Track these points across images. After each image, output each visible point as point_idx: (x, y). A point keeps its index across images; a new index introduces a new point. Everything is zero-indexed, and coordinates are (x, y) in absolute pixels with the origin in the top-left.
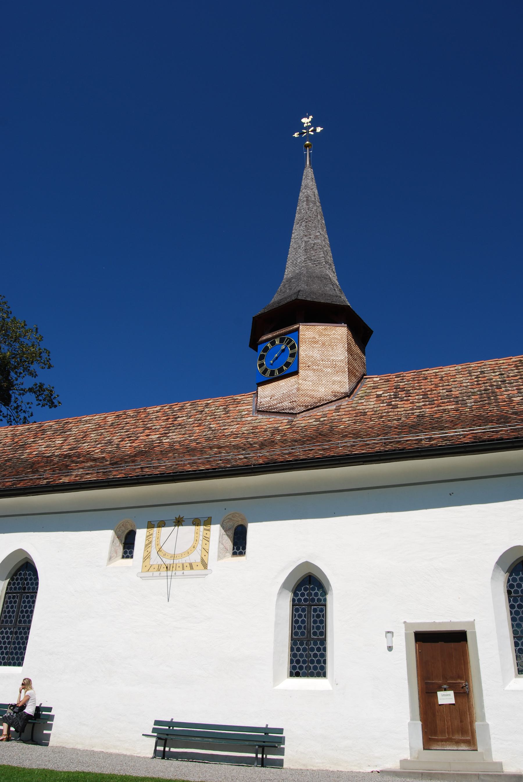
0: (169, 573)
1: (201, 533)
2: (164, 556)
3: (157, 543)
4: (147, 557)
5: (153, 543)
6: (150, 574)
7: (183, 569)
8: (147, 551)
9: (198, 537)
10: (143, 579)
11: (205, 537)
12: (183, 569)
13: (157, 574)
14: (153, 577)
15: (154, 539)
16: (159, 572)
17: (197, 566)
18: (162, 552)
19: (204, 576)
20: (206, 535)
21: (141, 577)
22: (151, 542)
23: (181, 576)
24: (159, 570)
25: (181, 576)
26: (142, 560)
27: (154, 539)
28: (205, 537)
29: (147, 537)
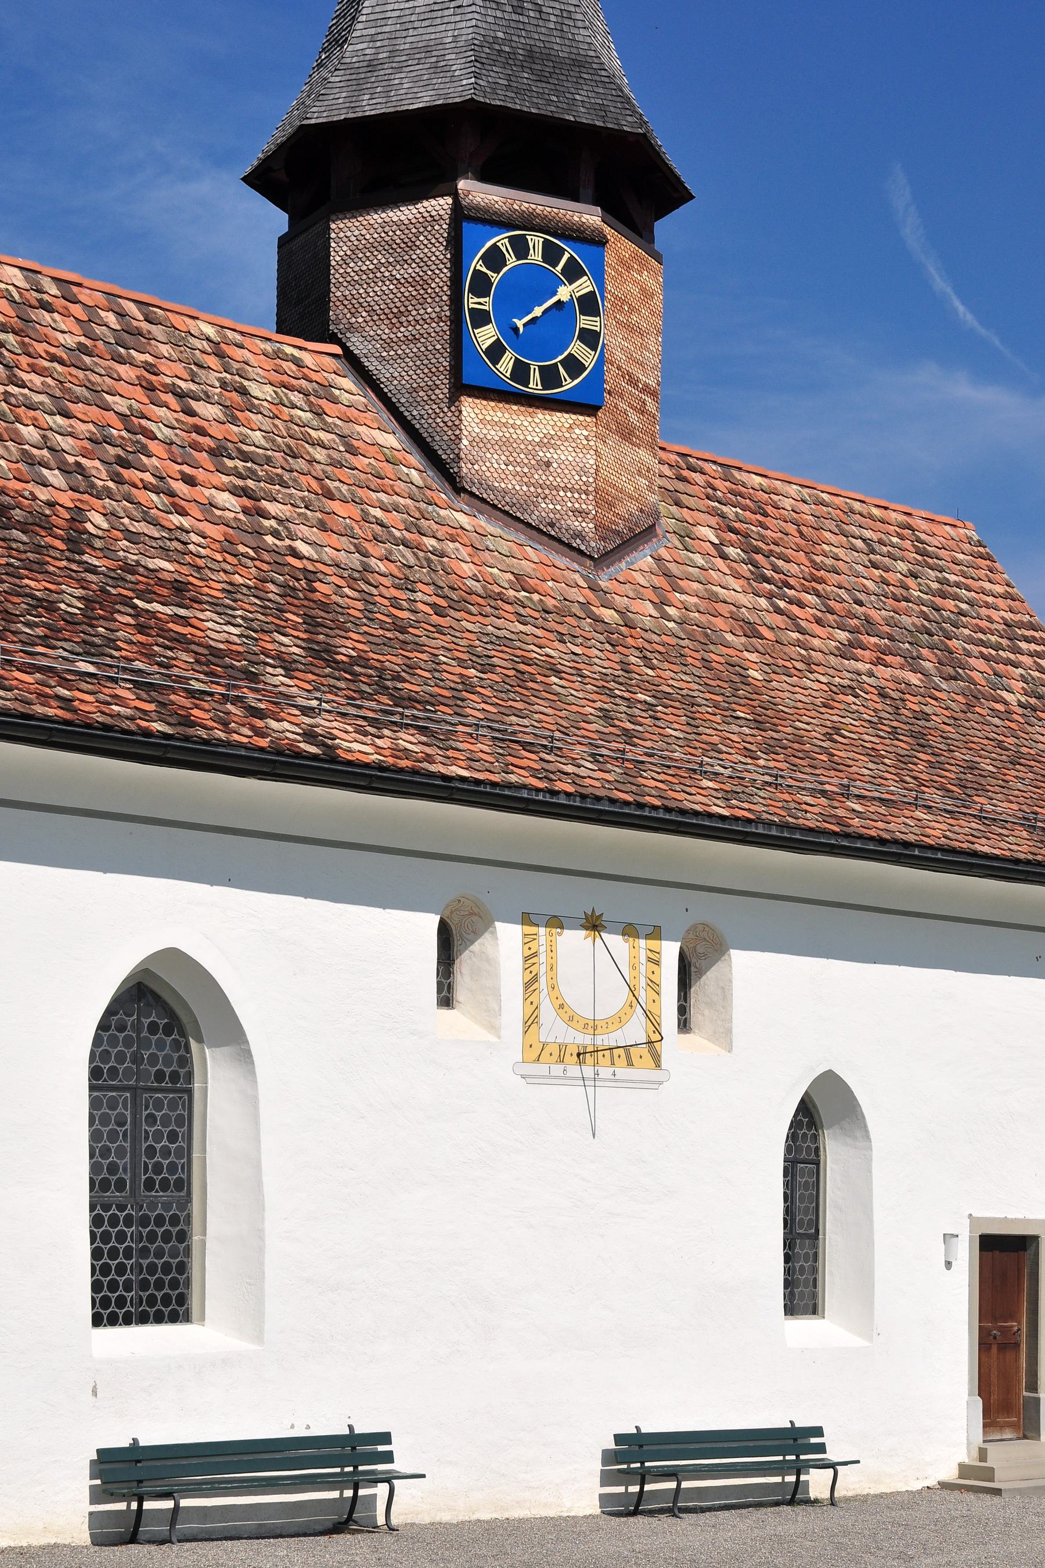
0: (588, 1071)
1: (643, 969)
2: (570, 1023)
3: (550, 982)
4: (531, 1022)
5: (543, 980)
6: (541, 1069)
7: (613, 1064)
8: (532, 1003)
9: (637, 978)
10: (529, 1080)
11: (651, 981)
12: (613, 1064)
13: (557, 1069)
14: (550, 1077)
15: (543, 969)
16: (561, 1067)
17: (641, 1057)
18: (564, 1010)
19: (656, 1086)
20: (653, 978)
21: (523, 1077)
22: (535, 979)
23: (610, 1080)
24: (561, 1060)
25: (610, 1080)
26: (520, 1027)
27: (543, 969)
28: (651, 981)
29: (526, 959)
